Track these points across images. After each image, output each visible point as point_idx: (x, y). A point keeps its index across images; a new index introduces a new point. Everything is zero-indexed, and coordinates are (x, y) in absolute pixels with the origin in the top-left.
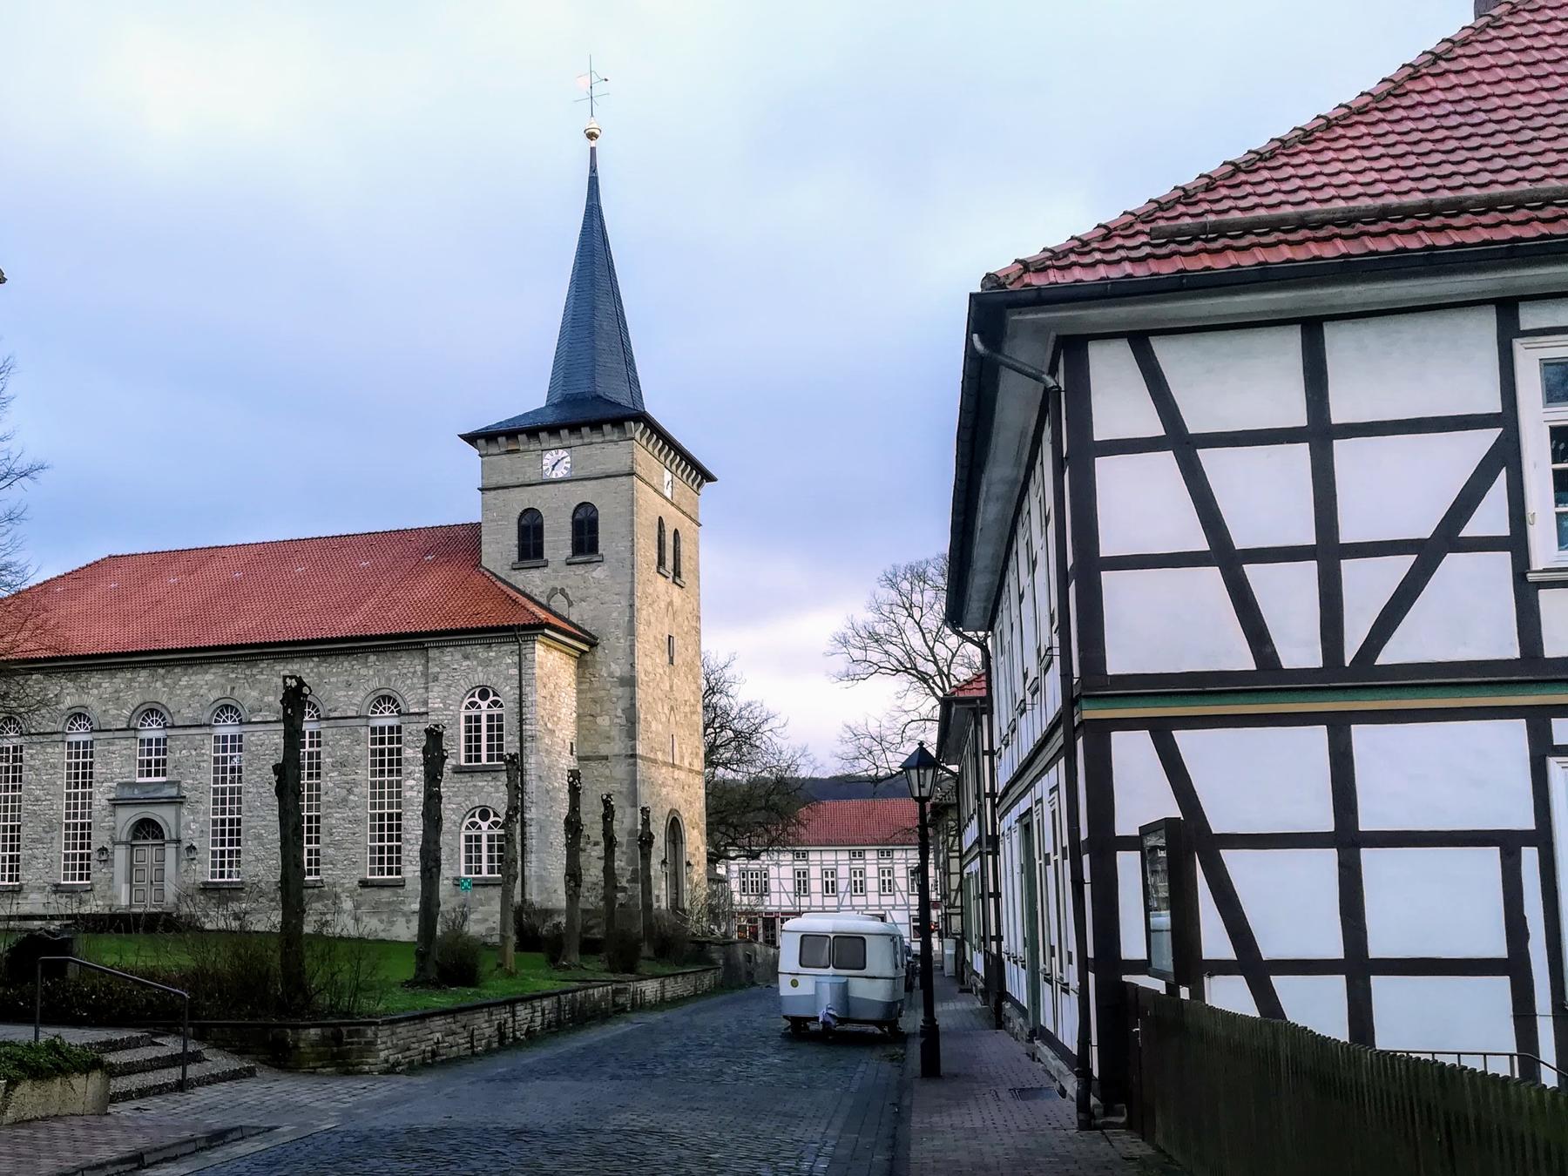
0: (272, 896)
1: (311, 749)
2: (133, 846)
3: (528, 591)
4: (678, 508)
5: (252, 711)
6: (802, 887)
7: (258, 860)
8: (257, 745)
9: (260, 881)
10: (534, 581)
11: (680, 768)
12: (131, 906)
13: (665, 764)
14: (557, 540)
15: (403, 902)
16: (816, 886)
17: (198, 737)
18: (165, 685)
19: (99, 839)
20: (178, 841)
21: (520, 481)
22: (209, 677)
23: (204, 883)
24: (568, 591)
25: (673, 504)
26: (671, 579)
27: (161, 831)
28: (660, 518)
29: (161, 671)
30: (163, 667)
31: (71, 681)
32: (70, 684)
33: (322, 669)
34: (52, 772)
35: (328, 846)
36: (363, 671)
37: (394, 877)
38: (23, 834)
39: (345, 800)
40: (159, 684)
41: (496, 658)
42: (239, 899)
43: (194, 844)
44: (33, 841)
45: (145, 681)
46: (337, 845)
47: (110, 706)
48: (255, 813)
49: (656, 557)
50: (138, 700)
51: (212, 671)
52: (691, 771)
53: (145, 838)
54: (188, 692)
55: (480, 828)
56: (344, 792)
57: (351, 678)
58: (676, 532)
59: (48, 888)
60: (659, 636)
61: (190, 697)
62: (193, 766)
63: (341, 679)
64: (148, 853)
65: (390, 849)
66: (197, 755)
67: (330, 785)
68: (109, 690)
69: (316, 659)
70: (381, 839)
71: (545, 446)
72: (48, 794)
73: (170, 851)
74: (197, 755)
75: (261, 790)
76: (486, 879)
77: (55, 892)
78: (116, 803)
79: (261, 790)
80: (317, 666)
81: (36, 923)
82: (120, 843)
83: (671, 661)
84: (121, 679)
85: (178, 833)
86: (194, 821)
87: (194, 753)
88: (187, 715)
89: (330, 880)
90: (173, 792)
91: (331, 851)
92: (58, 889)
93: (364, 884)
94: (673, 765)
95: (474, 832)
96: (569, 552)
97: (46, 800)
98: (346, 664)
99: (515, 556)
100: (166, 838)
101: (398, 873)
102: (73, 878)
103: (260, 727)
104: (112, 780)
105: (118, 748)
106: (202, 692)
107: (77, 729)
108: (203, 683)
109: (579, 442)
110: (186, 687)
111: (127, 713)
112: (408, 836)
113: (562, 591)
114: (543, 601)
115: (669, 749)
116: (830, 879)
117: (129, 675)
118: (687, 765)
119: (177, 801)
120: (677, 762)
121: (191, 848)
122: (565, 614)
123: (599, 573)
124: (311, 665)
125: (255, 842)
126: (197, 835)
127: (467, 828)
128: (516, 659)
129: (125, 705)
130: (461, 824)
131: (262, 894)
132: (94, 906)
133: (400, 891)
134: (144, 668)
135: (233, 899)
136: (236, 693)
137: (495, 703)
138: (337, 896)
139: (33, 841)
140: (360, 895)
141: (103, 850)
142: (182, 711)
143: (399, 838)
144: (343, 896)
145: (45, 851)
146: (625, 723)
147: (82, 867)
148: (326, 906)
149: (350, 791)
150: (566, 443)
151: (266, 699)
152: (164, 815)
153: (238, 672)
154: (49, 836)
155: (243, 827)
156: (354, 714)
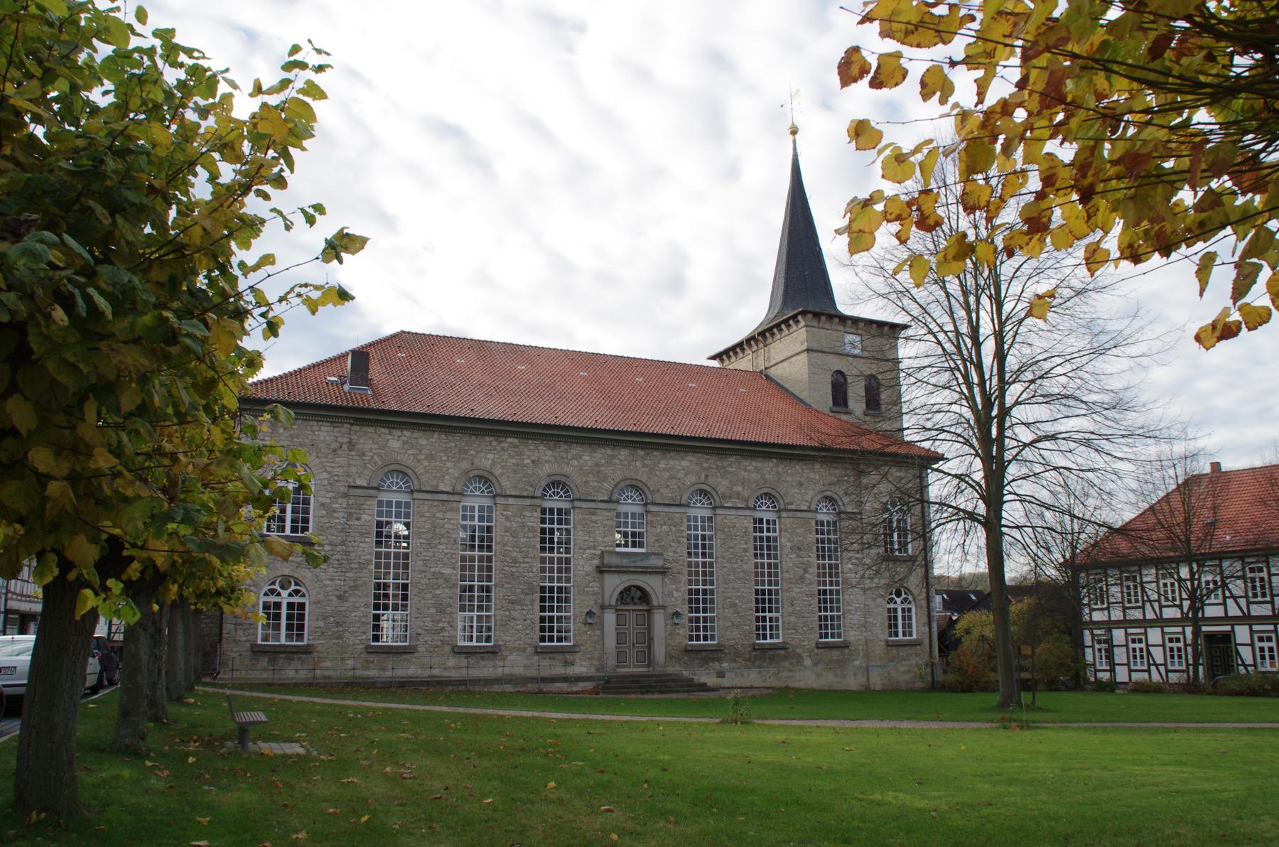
1: (768, 534)
5: (724, 497)
7: (733, 625)
8: (729, 527)
17: (677, 515)
18: (644, 466)
22: (684, 463)
29: (641, 452)
30: (642, 449)
31: (549, 449)
32: (549, 453)
33: (780, 470)
34: (530, 535)
36: (811, 475)
39: (802, 579)
40: (638, 464)
42: (719, 660)
43: (679, 610)
45: (625, 460)
47: (590, 478)
48: (730, 585)
50: (619, 476)
51: (689, 458)
54: (666, 475)
55: (895, 603)
56: (801, 571)
57: (803, 480)
59: (529, 649)
61: (668, 479)
62: (673, 541)
63: (795, 479)
66: (677, 531)
67: (791, 564)
68: (590, 463)
69: (775, 461)
72: (526, 556)
74: (677, 531)
75: (735, 566)
76: (901, 640)
77: (537, 653)
79: (735, 566)
80: (777, 466)
81: (557, 685)
82: (610, 607)
84: (601, 454)
87: (674, 529)
88: (666, 494)
90: (659, 563)
95: (892, 606)
97: (524, 562)
98: (798, 467)
100: (655, 603)
103: (733, 512)
104: (595, 548)
105: (600, 518)
106: (680, 475)
107: (550, 496)
108: (678, 467)
110: (664, 469)
111: (608, 486)
117: (609, 452)
119: (662, 572)
124: (771, 465)
125: (732, 610)
126: (678, 602)
129: (605, 479)
131: (738, 654)
133: (846, 651)
134: (624, 447)
135: (713, 660)
136: (710, 480)
140: (817, 654)
142: (661, 490)
144: (804, 655)
145: (524, 612)
149: (805, 571)
151: (735, 489)
152: (652, 584)
153: (711, 462)
154: (529, 597)
156: (806, 508)
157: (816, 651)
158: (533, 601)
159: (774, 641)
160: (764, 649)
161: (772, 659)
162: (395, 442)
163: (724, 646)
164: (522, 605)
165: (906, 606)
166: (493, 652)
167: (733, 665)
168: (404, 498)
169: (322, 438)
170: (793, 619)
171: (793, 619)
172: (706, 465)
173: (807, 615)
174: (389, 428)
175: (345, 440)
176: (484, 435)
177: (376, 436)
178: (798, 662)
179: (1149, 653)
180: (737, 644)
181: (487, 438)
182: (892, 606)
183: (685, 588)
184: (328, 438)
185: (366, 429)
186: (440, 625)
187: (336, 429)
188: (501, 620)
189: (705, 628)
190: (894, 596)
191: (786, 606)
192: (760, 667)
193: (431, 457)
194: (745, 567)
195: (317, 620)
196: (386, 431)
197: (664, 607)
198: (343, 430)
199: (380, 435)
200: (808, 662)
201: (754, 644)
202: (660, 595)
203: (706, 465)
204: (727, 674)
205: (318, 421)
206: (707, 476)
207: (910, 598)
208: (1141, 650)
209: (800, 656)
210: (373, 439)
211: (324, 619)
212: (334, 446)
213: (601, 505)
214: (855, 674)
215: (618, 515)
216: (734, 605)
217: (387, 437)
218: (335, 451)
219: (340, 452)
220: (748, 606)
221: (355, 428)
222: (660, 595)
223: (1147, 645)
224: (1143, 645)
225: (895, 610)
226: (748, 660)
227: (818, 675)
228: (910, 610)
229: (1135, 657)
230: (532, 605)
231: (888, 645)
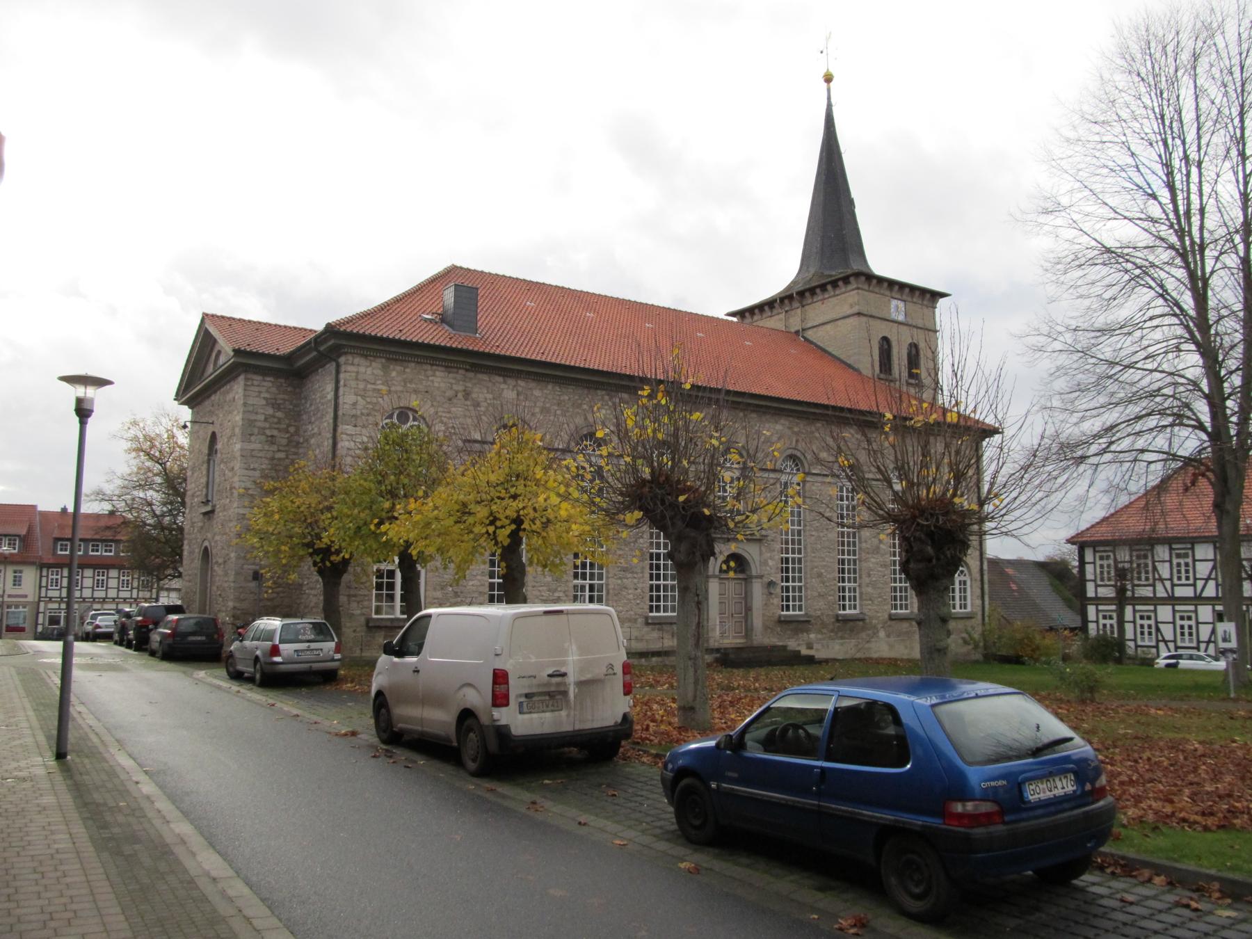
0: (831, 627)
7: (820, 595)
22: (779, 427)
39: (878, 548)
42: (808, 631)
51: (782, 421)
59: (640, 620)
75: (822, 534)
77: (647, 624)
86: (771, 558)
93: (892, 618)
100: (754, 573)
103: (820, 479)
126: (773, 571)
131: (824, 625)
135: (802, 631)
140: (890, 626)
145: (635, 581)
148: (868, 635)
153: (800, 426)
157: (889, 623)
158: (643, 568)
160: (846, 620)
161: (852, 630)
162: (509, 391)
163: (811, 616)
164: (633, 573)
167: (819, 636)
169: (436, 385)
170: (870, 590)
171: (870, 590)
172: (796, 429)
173: (881, 585)
174: (504, 376)
175: (461, 388)
176: (596, 389)
177: (490, 384)
179: (1158, 630)
180: (822, 614)
181: (599, 392)
183: (778, 556)
184: (442, 385)
185: (480, 376)
186: (556, 594)
187: (451, 375)
188: (614, 589)
191: (864, 576)
192: (842, 638)
193: (545, 410)
194: (829, 535)
195: (435, 589)
196: (501, 379)
197: (761, 577)
198: (459, 377)
199: (494, 384)
200: (882, 634)
201: (837, 616)
202: (758, 564)
203: (796, 429)
205: (432, 365)
206: (797, 441)
207: (966, 572)
208: (1150, 627)
209: (875, 627)
210: (488, 388)
211: (442, 589)
212: (449, 393)
216: (820, 575)
217: (503, 386)
218: (450, 400)
219: (455, 401)
220: (831, 576)
221: (471, 375)
222: (758, 564)
223: (1157, 622)
224: (1152, 622)
226: (832, 631)
227: (891, 646)
228: (965, 583)
229: (1182, 634)
230: (642, 572)
231: (838, 620)
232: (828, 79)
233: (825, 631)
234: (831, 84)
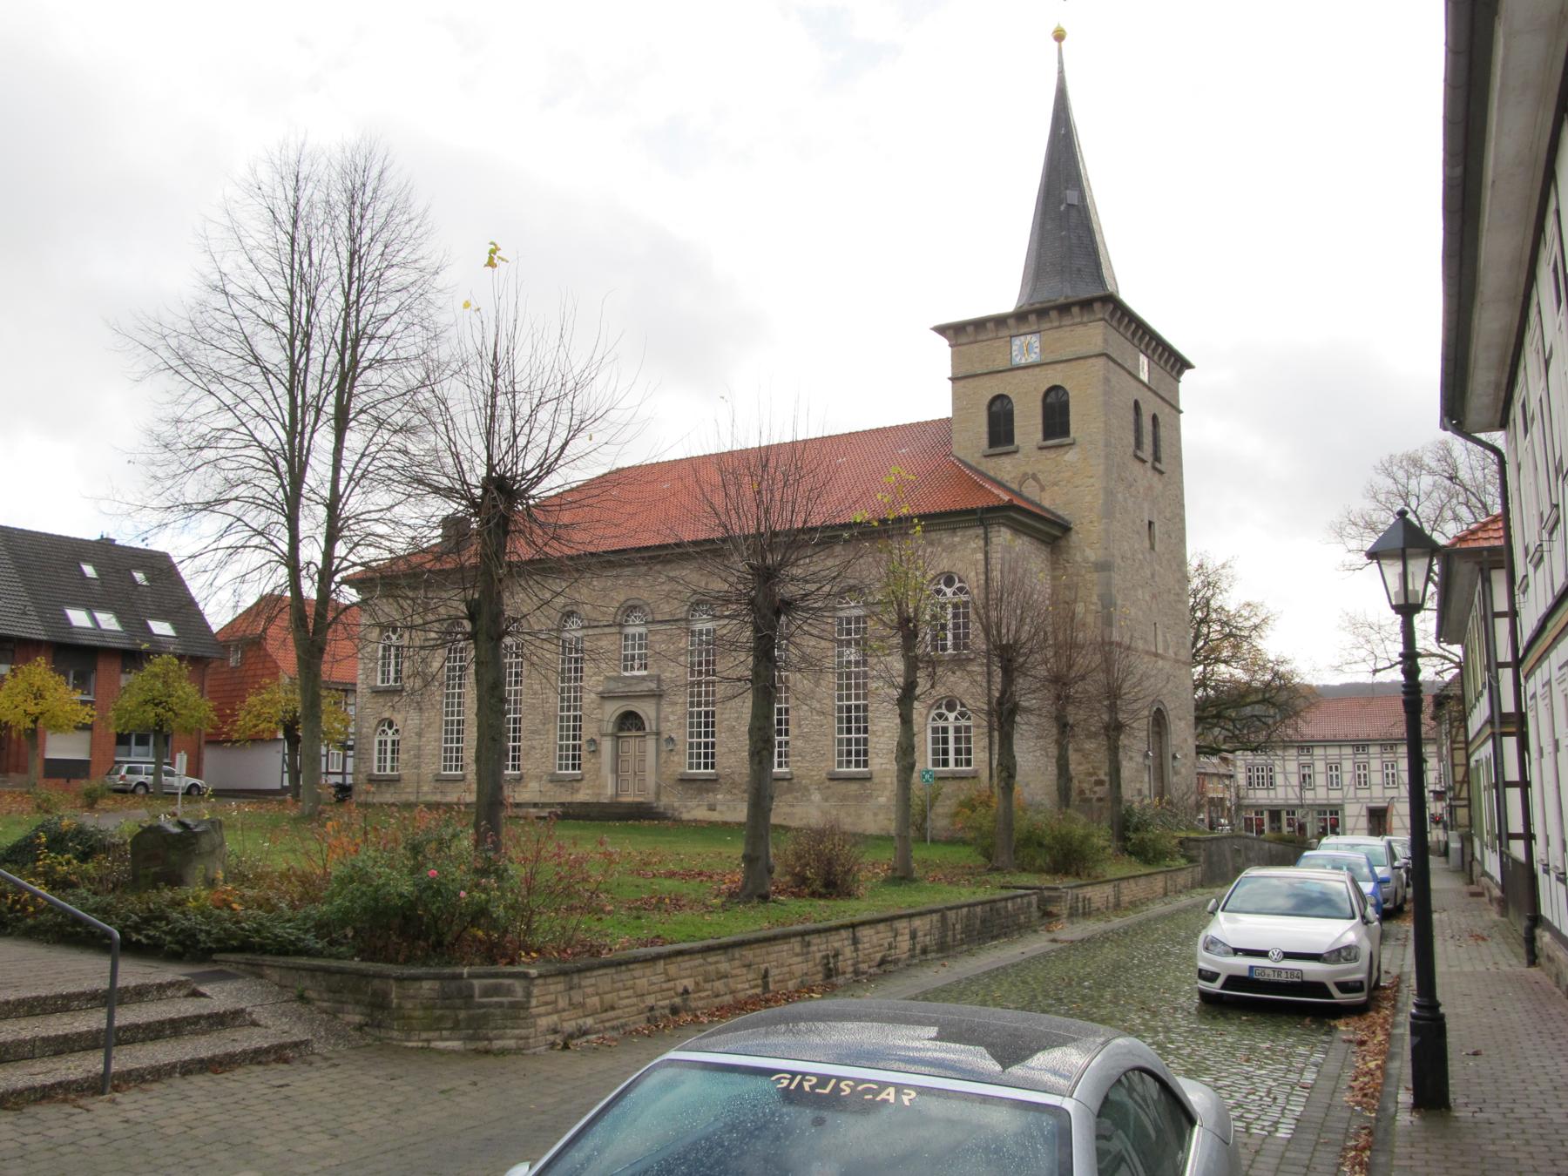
2: (618, 737)
3: (999, 478)
4: (1156, 393)
6: (1306, 781)
9: (733, 773)
10: (1005, 469)
11: (1163, 658)
12: (617, 795)
13: (1147, 652)
14: (1028, 424)
15: (870, 796)
16: (1320, 779)
19: (589, 731)
20: (658, 734)
21: (991, 368)
23: (681, 774)
24: (1040, 477)
25: (1150, 389)
26: (1149, 465)
27: (643, 723)
28: (1136, 403)
35: (797, 738)
37: (862, 769)
38: (523, 726)
41: (960, 543)
42: (714, 791)
44: (533, 732)
46: (804, 737)
49: (1132, 440)
52: (1177, 661)
53: (629, 730)
55: (946, 719)
58: (1155, 418)
60: (1138, 521)
64: (631, 745)
65: (857, 741)
70: (849, 731)
71: (1013, 332)
73: (651, 743)
76: (953, 772)
77: (551, 781)
78: (605, 697)
83: (1152, 547)
85: (658, 725)
86: (672, 713)
89: (799, 773)
90: (653, 686)
91: (800, 743)
92: (556, 780)
93: (834, 778)
94: (1156, 655)
95: (941, 723)
96: (1040, 435)
99: (985, 442)
100: (648, 730)
101: (866, 764)
102: (567, 768)
109: (1049, 325)
112: (875, 728)
113: (1034, 477)
114: (1015, 486)
115: (1151, 638)
116: (1334, 773)
118: (1171, 653)
120: (1160, 651)
121: (671, 739)
122: (1037, 499)
123: (1071, 456)
127: (934, 719)
128: (982, 543)
130: (928, 715)
131: (734, 785)
132: (583, 795)
133: (868, 784)
135: (708, 791)
137: (961, 590)
138: (806, 789)
139: (533, 732)
140: (829, 787)
141: (592, 741)
143: (866, 731)
146: (1100, 609)
147: (574, 757)
150: (1035, 328)
152: (646, 710)
155: (717, 719)
157: (827, 783)
159: (784, 769)
165: (963, 722)
166: (393, 781)
167: (728, 797)
168: (643, 630)
173: (816, 737)
178: (803, 795)
182: (941, 723)
189: (849, 753)
190: (944, 710)
200: (816, 797)
204: (718, 808)
209: (806, 789)
213: (607, 630)
214: (875, 815)
215: (626, 637)
225: (945, 730)
232: (1059, 36)
233: (735, 791)
234: (1063, 43)
